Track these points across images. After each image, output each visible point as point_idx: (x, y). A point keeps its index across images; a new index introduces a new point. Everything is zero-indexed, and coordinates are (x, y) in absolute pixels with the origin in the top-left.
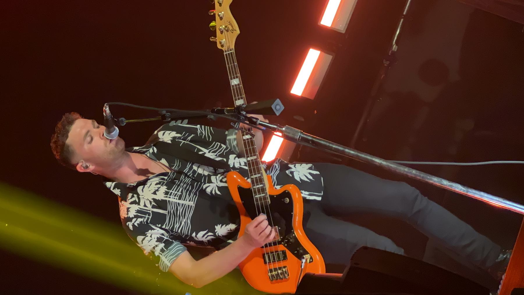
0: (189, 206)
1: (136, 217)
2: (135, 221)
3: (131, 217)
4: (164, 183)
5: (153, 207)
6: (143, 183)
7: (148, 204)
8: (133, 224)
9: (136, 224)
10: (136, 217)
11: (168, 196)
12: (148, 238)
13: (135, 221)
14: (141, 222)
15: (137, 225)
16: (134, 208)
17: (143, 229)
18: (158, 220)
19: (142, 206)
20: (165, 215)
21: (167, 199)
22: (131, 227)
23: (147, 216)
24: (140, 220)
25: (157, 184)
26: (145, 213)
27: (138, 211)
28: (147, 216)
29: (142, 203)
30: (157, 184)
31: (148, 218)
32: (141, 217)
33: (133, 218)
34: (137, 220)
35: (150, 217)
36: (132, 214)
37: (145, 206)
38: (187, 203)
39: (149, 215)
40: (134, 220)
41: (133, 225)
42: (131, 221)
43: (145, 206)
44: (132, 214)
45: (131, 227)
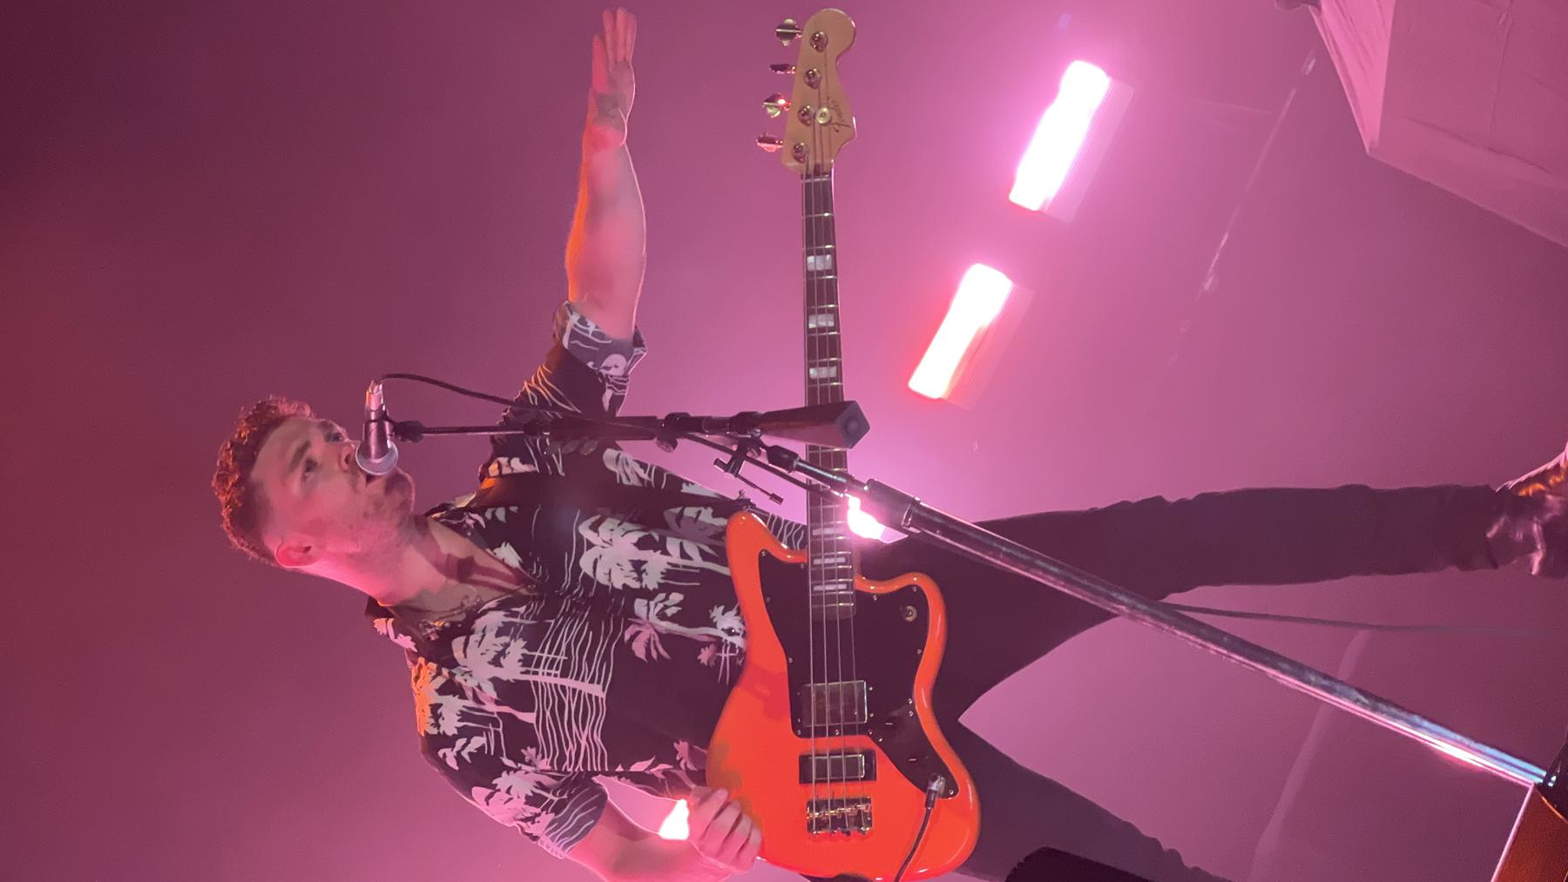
1: (465, 733)
2: (464, 747)
3: (449, 733)
4: (517, 630)
5: (497, 703)
8: (459, 753)
9: (465, 754)
10: (465, 733)
13: (464, 747)
16: (452, 707)
17: (482, 770)
18: (518, 739)
19: (470, 703)
24: (477, 742)
25: (498, 635)
27: (464, 716)
29: (469, 694)
33: (455, 737)
34: (468, 742)
36: (450, 725)
37: (476, 699)
39: (496, 725)
40: (460, 742)
41: (459, 757)
43: (476, 699)
44: (450, 725)
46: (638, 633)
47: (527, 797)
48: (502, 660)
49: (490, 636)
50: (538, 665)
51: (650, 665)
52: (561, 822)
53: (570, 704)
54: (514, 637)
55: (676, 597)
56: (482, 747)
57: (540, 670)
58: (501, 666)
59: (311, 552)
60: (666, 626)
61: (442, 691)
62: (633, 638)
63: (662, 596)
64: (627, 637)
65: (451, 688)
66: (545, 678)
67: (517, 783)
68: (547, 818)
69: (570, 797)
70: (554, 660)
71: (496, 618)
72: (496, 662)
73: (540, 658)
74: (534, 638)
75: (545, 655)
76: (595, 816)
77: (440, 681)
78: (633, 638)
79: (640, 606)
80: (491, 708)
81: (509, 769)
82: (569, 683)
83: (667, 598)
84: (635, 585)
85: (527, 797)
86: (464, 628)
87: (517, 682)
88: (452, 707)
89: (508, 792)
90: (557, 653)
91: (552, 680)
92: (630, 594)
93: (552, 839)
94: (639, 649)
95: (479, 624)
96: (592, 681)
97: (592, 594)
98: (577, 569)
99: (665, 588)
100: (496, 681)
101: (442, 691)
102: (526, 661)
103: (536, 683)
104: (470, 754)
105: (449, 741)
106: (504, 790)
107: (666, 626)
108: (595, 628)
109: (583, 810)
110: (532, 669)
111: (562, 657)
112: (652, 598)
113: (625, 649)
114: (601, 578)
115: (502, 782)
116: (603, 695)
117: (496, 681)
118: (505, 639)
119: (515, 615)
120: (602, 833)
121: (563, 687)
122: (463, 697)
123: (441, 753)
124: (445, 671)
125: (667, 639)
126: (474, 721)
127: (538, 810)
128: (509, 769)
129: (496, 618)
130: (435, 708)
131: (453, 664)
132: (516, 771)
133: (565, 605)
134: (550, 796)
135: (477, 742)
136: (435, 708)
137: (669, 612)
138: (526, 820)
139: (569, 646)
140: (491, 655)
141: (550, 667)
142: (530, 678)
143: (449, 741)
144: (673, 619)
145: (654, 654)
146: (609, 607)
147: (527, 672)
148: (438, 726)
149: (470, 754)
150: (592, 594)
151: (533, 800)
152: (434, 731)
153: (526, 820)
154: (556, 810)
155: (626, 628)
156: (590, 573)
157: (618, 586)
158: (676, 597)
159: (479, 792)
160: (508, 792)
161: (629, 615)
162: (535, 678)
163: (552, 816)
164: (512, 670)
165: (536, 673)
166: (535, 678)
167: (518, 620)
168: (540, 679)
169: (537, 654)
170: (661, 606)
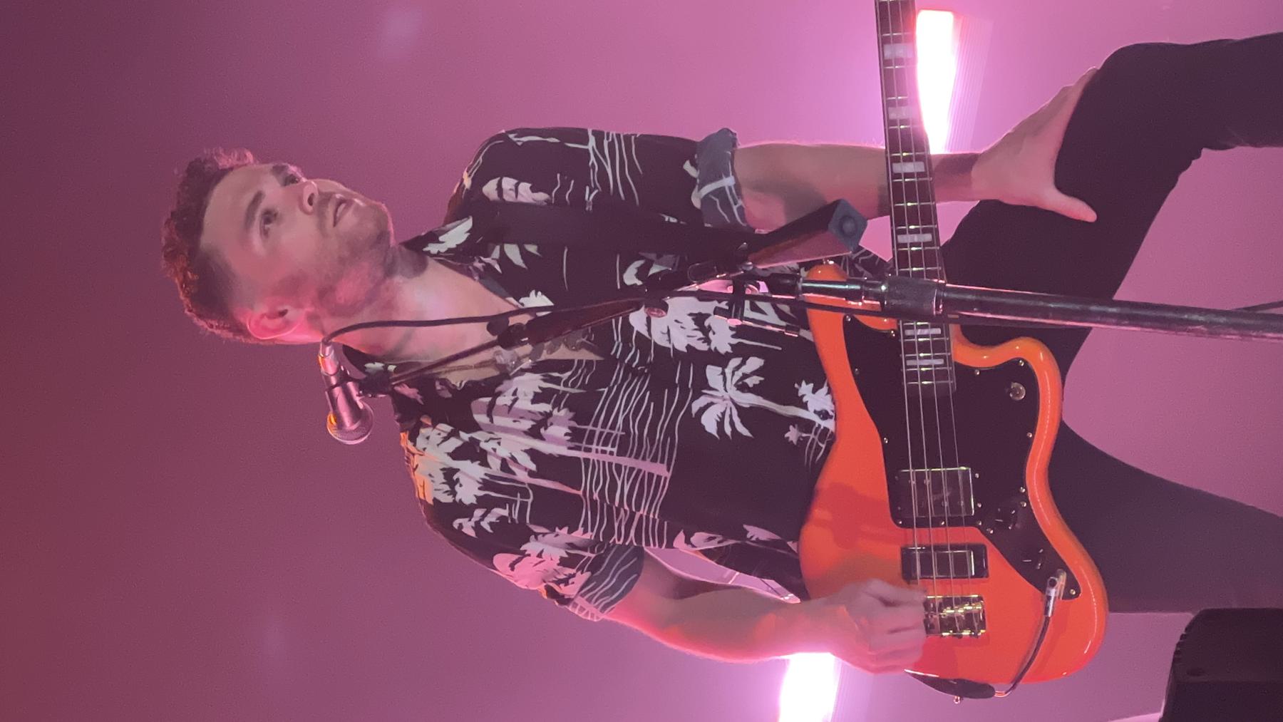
5: (531, 474)
8: (478, 523)
9: (485, 525)
14: (502, 518)
15: (488, 528)
16: (471, 477)
17: (511, 538)
18: (555, 511)
23: (519, 499)
26: (512, 491)
27: (485, 485)
29: (495, 464)
30: (537, 399)
31: (523, 506)
32: (501, 503)
35: (530, 501)
36: (468, 493)
37: (504, 465)
40: (478, 513)
41: (478, 527)
42: (470, 516)
44: (468, 493)
45: (468, 529)
46: (712, 404)
47: (562, 559)
48: (542, 430)
49: (524, 404)
50: (590, 441)
52: (600, 580)
54: (556, 405)
55: (755, 363)
57: (594, 447)
58: (541, 438)
59: (288, 316)
60: (749, 400)
61: (456, 455)
62: (703, 410)
63: (735, 362)
64: (696, 406)
65: (471, 452)
66: (598, 454)
67: (547, 548)
68: (582, 578)
69: (608, 550)
70: (609, 435)
71: (530, 383)
72: (534, 433)
73: (592, 433)
74: (582, 409)
75: (598, 430)
76: (636, 570)
77: (454, 443)
78: (703, 410)
79: (713, 373)
80: (522, 476)
81: (536, 535)
82: (626, 461)
83: (743, 363)
84: (703, 347)
85: (562, 559)
86: (490, 388)
87: (562, 457)
88: (471, 472)
89: (540, 555)
90: (613, 427)
91: (607, 458)
92: (699, 359)
93: (589, 600)
94: (709, 423)
95: (508, 387)
96: (654, 460)
97: (651, 358)
98: (628, 327)
99: (741, 352)
100: (533, 453)
101: (456, 455)
102: (576, 436)
103: (587, 460)
104: (491, 524)
105: (466, 511)
107: (749, 400)
108: (656, 398)
109: (623, 564)
110: (584, 444)
111: (618, 432)
112: (724, 366)
113: (693, 422)
114: (658, 338)
115: (531, 547)
116: (669, 475)
117: (533, 453)
118: (545, 407)
119: (557, 381)
120: (645, 592)
121: (619, 467)
122: (485, 463)
123: (456, 524)
124: (465, 436)
125: (746, 414)
126: (498, 489)
127: (572, 571)
129: (530, 383)
130: (449, 474)
131: (476, 427)
132: (544, 534)
133: (618, 373)
134: (588, 554)
136: (449, 474)
137: (753, 381)
138: (559, 582)
139: (626, 420)
140: (527, 424)
141: (605, 444)
142: (580, 454)
143: (466, 511)
144: (755, 390)
145: (728, 430)
146: (678, 373)
147: (578, 448)
148: (453, 493)
149: (491, 524)
150: (651, 358)
151: (563, 562)
152: (449, 499)
153: (559, 582)
154: (594, 566)
155: (695, 398)
156: (646, 334)
157: (681, 347)
158: (755, 363)
159: (502, 561)
160: (540, 555)
161: (702, 385)
162: (586, 455)
163: (587, 575)
164: (556, 442)
165: (589, 450)
166: (586, 455)
167: (561, 388)
168: (592, 456)
169: (590, 427)
170: (739, 374)
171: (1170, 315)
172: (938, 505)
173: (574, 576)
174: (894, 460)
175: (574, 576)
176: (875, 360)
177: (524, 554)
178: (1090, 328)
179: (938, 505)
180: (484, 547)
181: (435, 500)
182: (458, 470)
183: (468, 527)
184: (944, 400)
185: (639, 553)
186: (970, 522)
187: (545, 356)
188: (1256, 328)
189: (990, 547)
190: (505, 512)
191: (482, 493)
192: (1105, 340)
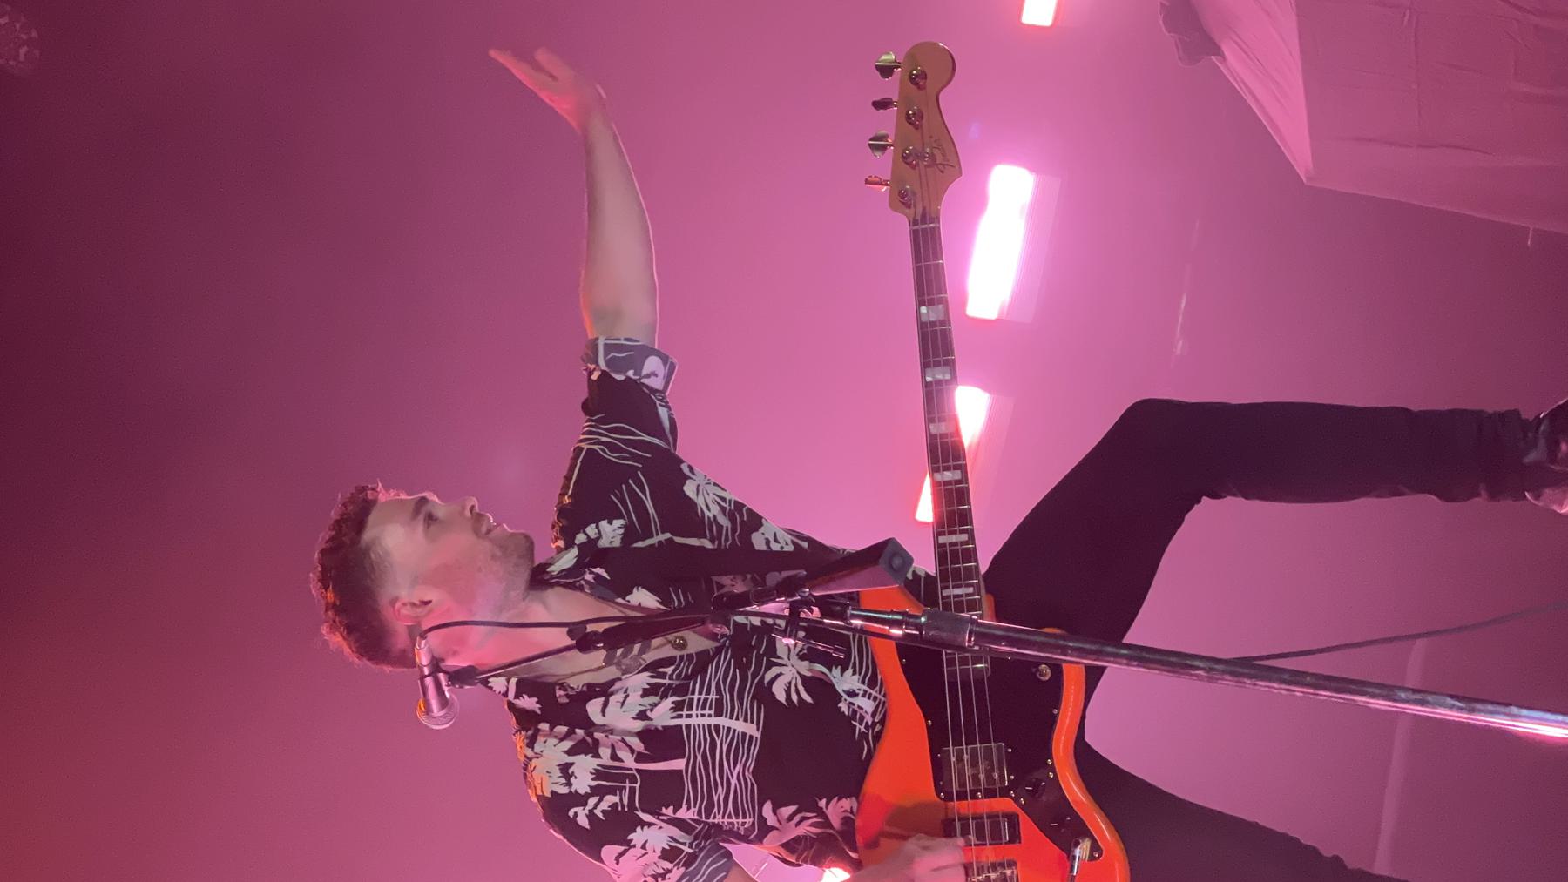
0: (744, 735)
1: (599, 792)
2: (597, 805)
3: (582, 792)
6: (603, 691)
7: (624, 754)
8: (591, 811)
9: (598, 812)
10: (599, 792)
11: (685, 713)
12: (638, 851)
13: (597, 805)
17: (616, 828)
20: (677, 774)
21: (683, 722)
22: (583, 821)
23: (628, 785)
27: (599, 774)
28: (628, 785)
29: (605, 752)
32: (612, 791)
33: (588, 796)
34: (601, 800)
36: (583, 783)
37: (614, 757)
38: (740, 726)
40: (592, 801)
41: (591, 816)
42: (585, 805)
45: (583, 821)
46: (780, 674)
51: (794, 709)
52: (693, 875)
53: (722, 744)
56: (614, 806)
89: (644, 847)
94: (781, 696)
104: (603, 812)
105: (581, 800)
106: (639, 845)
113: (764, 694)
115: (637, 836)
123: (571, 814)
127: (668, 865)
128: (643, 824)
130: (565, 769)
132: (650, 824)
135: (610, 799)
136: (565, 769)
143: (581, 800)
145: (795, 698)
148: (569, 784)
149: (603, 812)
152: (564, 790)
154: (687, 865)
155: (768, 669)
159: (610, 851)
160: (644, 847)
163: (682, 870)
171: (1174, 659)
172: (975, 777)
173: (670, 871)
174: (937, 741)
175: (670, 871)
176: (921, 663)
177: (629, 845)
178: (1104, 668)
179: (975, 777)
180: (594, 838)
181: (553, 793)
182: (572, 764)
183: (581, 816)
184: (979, 682)
185: (728, 854)
186: (1004, 792)
187: (650, 657)
188: (1250, 677)
189: (1023, 817)
190: (616, 799)
191: (594, 783)
192: (1116, 674)
